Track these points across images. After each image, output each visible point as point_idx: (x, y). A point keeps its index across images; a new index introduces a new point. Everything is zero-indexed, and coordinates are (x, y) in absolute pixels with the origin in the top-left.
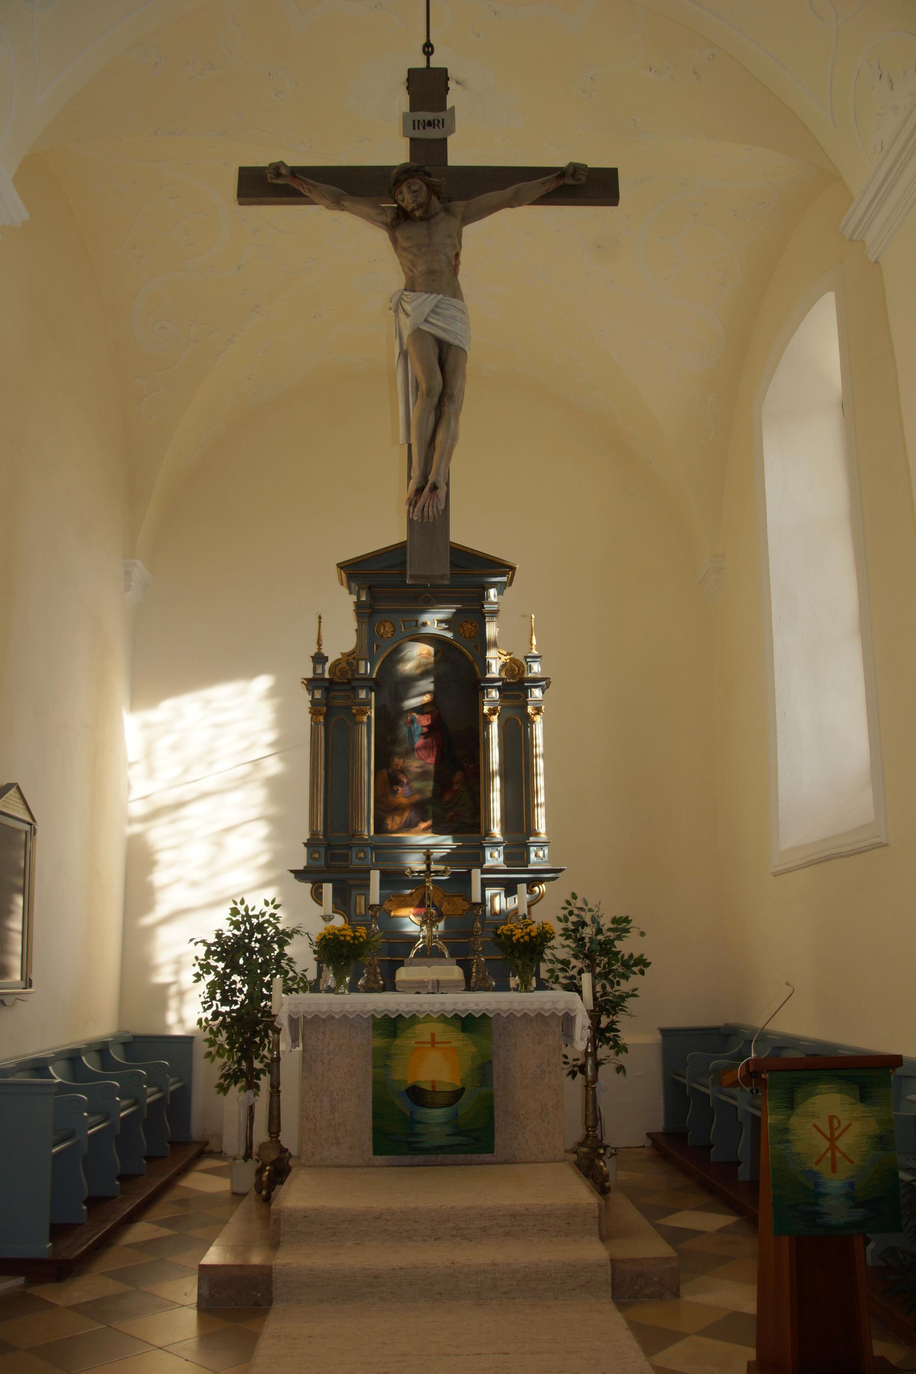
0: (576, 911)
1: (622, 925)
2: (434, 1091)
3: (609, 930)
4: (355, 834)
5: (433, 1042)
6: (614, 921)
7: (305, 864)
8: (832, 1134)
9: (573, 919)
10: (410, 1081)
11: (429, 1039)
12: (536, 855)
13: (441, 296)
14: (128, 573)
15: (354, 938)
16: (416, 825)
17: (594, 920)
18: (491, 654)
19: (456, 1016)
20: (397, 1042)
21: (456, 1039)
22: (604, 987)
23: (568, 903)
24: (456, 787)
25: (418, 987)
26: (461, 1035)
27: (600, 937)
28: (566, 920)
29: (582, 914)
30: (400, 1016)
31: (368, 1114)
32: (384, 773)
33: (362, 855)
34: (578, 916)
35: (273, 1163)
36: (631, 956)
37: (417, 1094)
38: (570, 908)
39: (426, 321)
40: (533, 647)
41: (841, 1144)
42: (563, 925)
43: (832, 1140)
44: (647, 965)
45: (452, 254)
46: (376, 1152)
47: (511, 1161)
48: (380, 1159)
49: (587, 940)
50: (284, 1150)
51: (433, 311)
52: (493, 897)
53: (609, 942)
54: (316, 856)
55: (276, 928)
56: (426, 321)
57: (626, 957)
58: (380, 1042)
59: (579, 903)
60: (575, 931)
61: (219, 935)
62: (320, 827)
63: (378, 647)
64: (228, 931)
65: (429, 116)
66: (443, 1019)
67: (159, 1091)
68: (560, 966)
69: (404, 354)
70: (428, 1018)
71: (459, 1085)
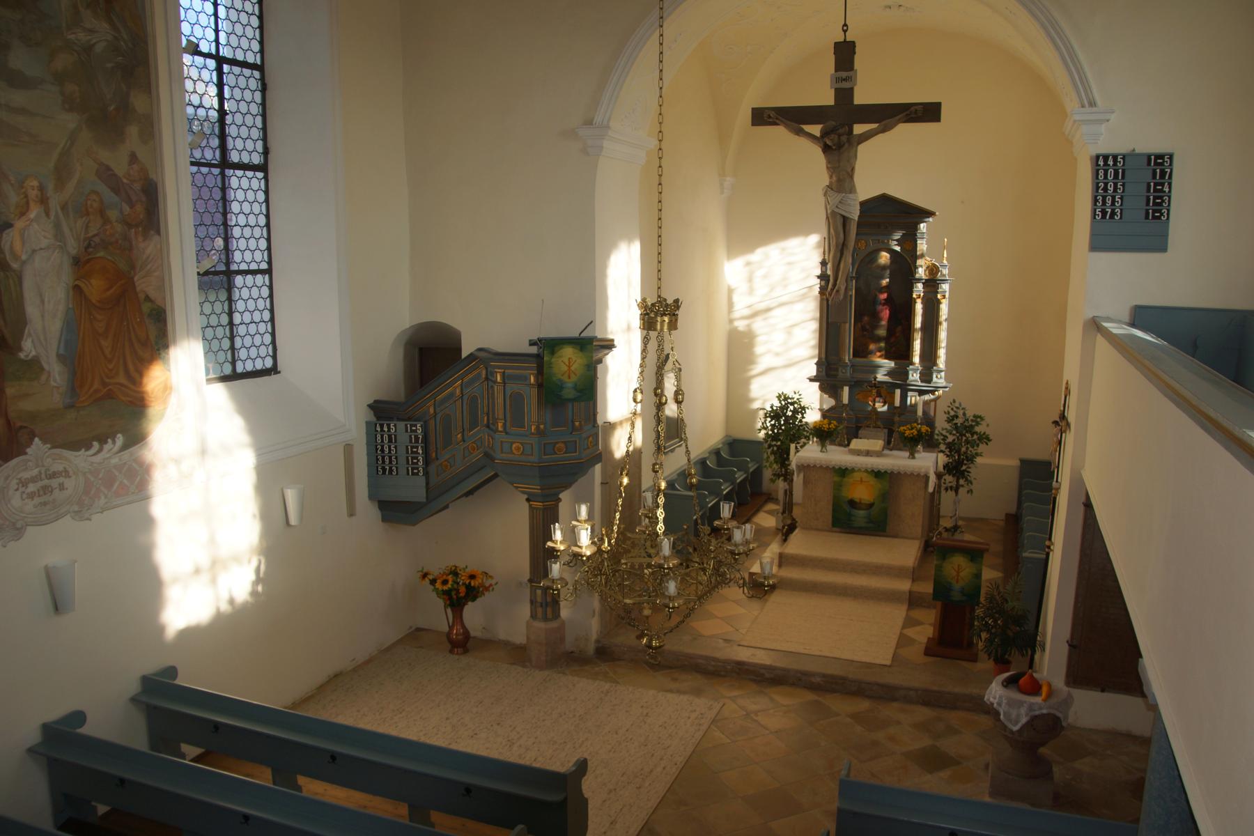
0: (955, 409)
1: (978, 419)
2: (860, 503)
3: (972, 420)
4: (840, 360)
5: (861, 481)
6: (974, 416)
7: (815, 374)
8: (959, 570)
9: (952, 413)
10: (850, 497)
11: (859, 479)
12: (937, 377)
13: (844, 194)
14: (722, 185)
15: (829, 428)
16: (875, 354)
17: (964, 414)
18: (919, 262)
19: (873, 471)
20: (846, 479)
21: (872, 480)
22: (967, 448)
23: (951, 404)
24: (898, 334)
25: (858, 453)
26: (875, 479)
27: (966, 424)
28: (949, 413)
29: (958, 411)
30: (846, 469)
31: (831, 508)
32: (859, 325)
33: (844, 371)
34: (955, 412)
35: (788, 526)
36: (984, 433)
37: (852, 503)
38: (952, 407)
39: (837, 207)
40: (945, 259)
41: (962, 574)
42: (947, 415)
43: (958, 573)
44: (990, 440)
45: (849, 170)
46: (834, 525)
47: (895, 536)
48: (835, 529)
49: (959, 425)
50: (794, 519)
51: (840, 202)
52: (911, 397)
53: (972, 427)
54: (821, 370)
55: (800, 405)
56: (837, 207)
57: (982, 433)
58: (837, 479)
59: (957, 405)
60: (953, 420)
61: (772, 407)
62: (823, 356)
63: (857, 255)
64: (777, 404)
65: (844, 74)
66: (866, 471)
67: (745, 473)
68: (942, 437)
69: (827, 218)
70: (859, 470)
71: (872, 501)
